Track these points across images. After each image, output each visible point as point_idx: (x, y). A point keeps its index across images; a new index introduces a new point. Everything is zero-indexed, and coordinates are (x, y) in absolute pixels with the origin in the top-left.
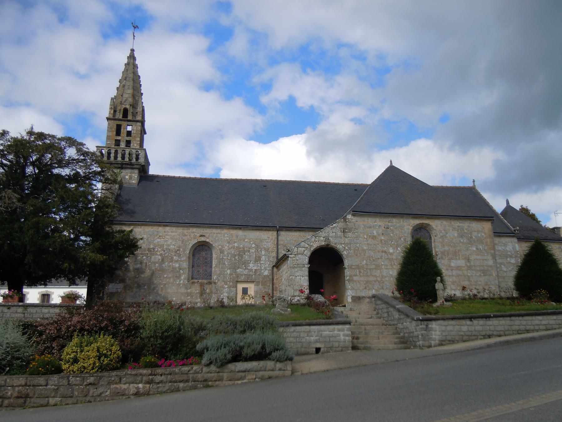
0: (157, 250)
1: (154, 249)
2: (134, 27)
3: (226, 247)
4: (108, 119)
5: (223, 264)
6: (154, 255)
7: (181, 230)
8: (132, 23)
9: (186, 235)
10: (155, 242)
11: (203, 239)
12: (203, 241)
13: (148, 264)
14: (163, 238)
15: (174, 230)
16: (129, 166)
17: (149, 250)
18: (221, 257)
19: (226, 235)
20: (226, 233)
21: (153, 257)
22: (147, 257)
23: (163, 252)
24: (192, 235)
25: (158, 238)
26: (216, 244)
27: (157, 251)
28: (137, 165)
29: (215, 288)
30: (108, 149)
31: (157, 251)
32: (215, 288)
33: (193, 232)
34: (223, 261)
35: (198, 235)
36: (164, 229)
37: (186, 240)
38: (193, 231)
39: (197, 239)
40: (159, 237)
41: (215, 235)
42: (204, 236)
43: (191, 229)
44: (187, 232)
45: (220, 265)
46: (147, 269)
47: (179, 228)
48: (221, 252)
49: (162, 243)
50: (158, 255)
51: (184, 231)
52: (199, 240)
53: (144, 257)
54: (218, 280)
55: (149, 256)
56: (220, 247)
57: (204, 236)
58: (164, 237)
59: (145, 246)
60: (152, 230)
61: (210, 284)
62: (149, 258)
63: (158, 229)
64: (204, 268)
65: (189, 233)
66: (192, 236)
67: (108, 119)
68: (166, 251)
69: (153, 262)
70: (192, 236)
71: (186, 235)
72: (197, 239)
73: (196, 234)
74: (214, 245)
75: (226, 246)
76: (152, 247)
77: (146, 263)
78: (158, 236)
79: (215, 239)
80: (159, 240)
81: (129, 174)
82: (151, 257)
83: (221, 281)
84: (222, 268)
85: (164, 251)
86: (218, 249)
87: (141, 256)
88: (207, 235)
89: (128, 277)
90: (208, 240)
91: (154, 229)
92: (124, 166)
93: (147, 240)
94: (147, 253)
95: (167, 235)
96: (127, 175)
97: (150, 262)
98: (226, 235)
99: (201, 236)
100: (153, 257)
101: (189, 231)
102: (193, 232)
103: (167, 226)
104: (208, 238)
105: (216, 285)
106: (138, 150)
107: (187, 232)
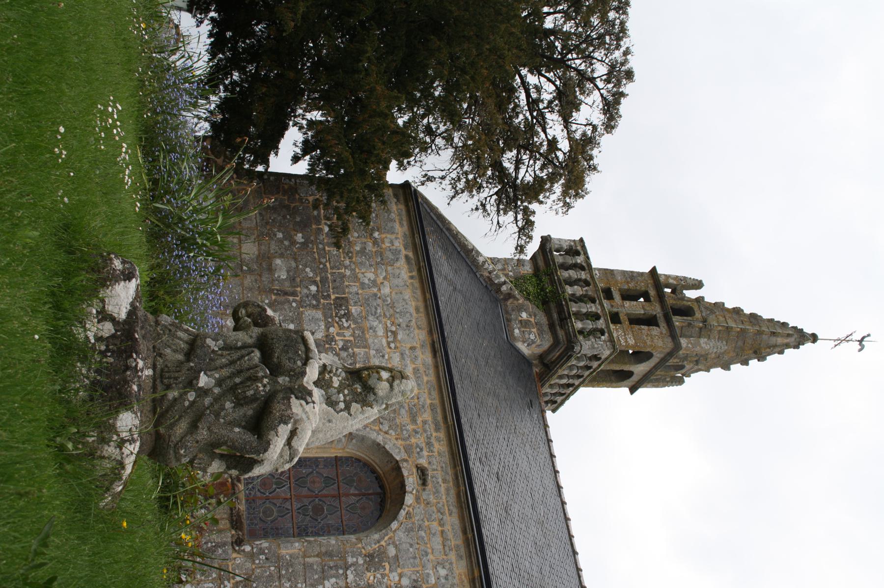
0: (346, 325)
1: (348, 316)
2: (863, 338)
3: (395, 577)
4: (654, 271)
5: (323, 571)
6: (325, 316)
7: (428, 402)
8: (869, 335)
9: (414, 420)
10: (371, 318)
11: (411, 481)
12: (404, 481)
13: (291, 298)
14: (389, 343)
15: (425, 379)
16: (555, 316)
17: (341, 302)
18: (350, 560)
19: (443, 572)
20: (451, 570)
21: (319, 314)
22: (315, 297)
23: (341, 344)
24: (419, 440)
25: (387, 330)
26: (401, 534)
27: (341, 327)
28: (567, 334)
29: (218, 546)
30: (584, 264)
31: (341, 327)
32: (218, 546)
33: (429, 444)
34: (337, 567)
35: (423, 462)
36: (422, 346)
37: (398, 421)
38: (433, 440)
39: (406, 461)
40: (392, 332)
41: (435, 525)
42: (424, 483)
43: (442, 435)
44: (425, 422)
45: (317, 556)
46: (274, 297)
47: (435, 394)
48: (371, 556)
49: (370, 341)
50: (327, 329)
51: (428, 410)
52: (404, 466)
53: (313, 288)
54: (252, 556)
55: (319, 302)
56: (392, 551)
57: (424, 483)
58: (392, 345)
59: (354, 289)
60: (412, 310)
61: (231, 521)
62: (314, 302)
63: (419, 328)
64: (296, 505)
65: (425, 431)
66: (413, 440)
67: (654, 271)
68: (344, 354)
69: (302, 313)
70: (413, 440)
71: (414, 420)
72: (406, 461)
73: (425, 453)
74: (394, 525)
75: (401, 576)
76: (354, 310)
77: (294, 294)
78: (394, 329)
79: (420, 527)
80: (381, 332)
81: (532, 320)
82: (316, 307)
83: (249, 565)
84: (307, 567)
85: (344, 348)
86: (383, 543)
87: (318, 279)
88: (428, 495)
89: (240, 241)
90: (409, 499)
91: (415, 315)
92: (552, 305)
93: (375, 295)
94: (329, 296)
95: (402, 354)
96: (530, 316)
97: (301, 304)
98: (443, 572)
99: (422, 472)
100: (319, 314)
101: (430, 428)
102: (429, 444)
103: (434, 352)
104: (418, 499)
105: (229, 548)
106: (606, 334)
107: (425, 422)
